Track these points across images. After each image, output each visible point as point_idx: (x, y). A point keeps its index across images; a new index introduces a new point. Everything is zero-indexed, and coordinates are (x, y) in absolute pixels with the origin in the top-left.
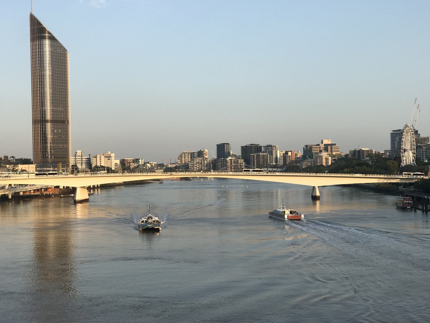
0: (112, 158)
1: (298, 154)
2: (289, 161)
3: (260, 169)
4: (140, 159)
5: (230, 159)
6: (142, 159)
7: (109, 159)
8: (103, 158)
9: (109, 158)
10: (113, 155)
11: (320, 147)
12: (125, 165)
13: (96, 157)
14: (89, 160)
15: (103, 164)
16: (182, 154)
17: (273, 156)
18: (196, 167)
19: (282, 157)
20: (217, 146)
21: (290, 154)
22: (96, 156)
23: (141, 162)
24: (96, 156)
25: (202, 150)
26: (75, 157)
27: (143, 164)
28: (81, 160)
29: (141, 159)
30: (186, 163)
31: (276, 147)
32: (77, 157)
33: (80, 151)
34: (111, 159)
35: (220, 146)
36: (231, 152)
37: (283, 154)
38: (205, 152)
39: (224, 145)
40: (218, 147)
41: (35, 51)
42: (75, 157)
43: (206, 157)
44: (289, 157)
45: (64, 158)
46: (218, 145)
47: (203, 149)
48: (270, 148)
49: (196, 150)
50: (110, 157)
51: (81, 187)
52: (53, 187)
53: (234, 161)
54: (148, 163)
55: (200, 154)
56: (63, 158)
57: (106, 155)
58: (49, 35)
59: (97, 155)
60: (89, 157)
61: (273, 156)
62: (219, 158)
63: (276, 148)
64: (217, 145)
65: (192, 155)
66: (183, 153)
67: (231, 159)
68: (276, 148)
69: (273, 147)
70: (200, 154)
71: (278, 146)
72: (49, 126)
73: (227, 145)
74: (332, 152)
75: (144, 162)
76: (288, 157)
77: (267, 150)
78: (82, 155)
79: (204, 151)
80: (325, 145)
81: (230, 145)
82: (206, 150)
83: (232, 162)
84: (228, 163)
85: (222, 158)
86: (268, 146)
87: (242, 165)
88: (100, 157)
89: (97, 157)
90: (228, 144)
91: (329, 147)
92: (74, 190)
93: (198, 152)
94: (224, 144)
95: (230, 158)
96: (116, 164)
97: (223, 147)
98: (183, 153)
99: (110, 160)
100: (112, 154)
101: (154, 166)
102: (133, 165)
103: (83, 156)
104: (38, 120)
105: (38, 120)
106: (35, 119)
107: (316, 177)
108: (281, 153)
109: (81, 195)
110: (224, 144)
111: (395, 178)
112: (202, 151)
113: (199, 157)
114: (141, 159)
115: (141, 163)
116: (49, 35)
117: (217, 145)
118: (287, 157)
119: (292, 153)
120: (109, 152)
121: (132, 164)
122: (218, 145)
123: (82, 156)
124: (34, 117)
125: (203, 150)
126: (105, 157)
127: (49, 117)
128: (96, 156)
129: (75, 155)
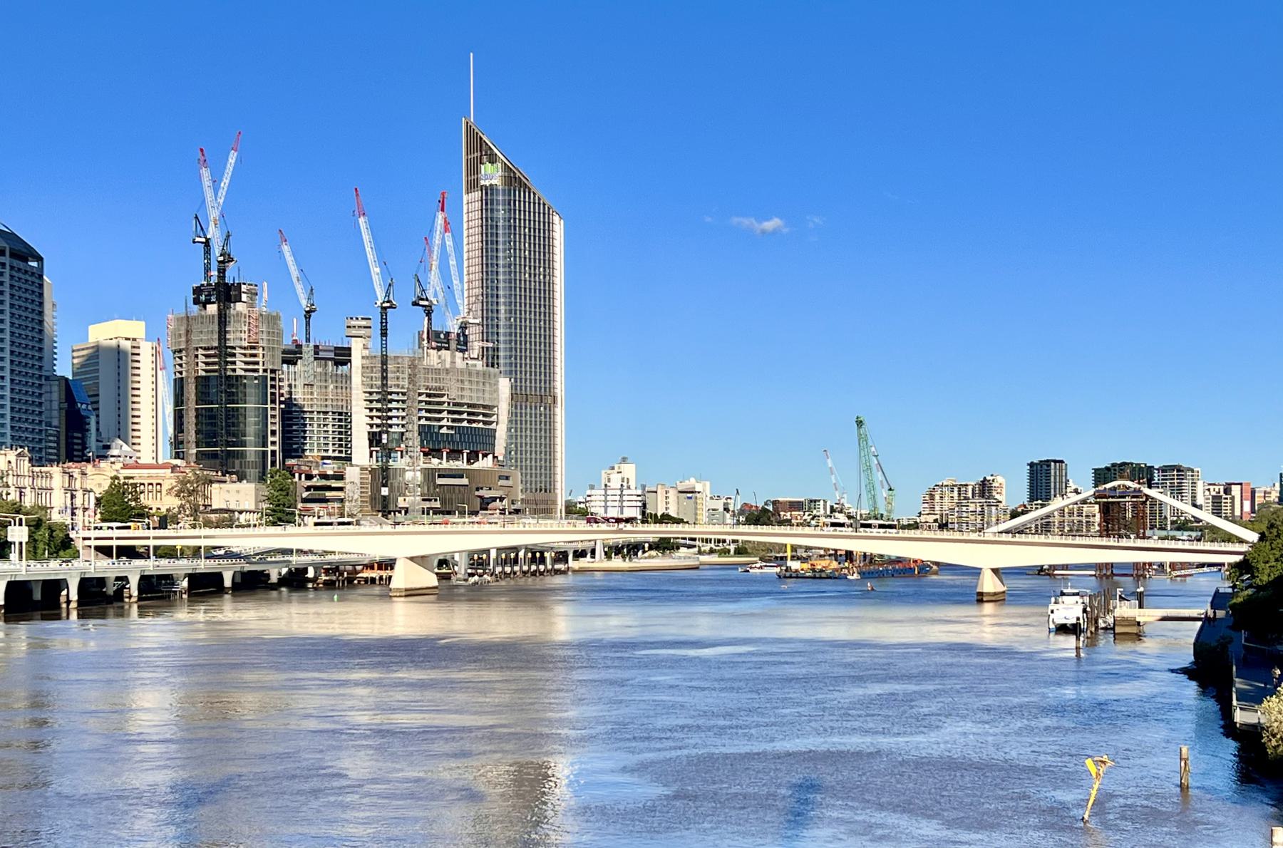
1: (1270, 493)
2: (1229, 511)
4: (819, 501)
7: (690, 498)
14: (640, 498)
15: (673, 513)
17: (1182, 496)
19: (1208, 499)
20: (1028, 467)
21: (1236, 490)
25: (988, 478)
27: (828, 513)
28: (625, 498)
30: (944, 513)
31: (1193, 471)
35: (1039, 467)
36: (1070, 483)
37: (1217, 490)
39: (1049, 466)
42: (606, 490)
43: (997, 496)
44: (1229, 501)
46: (1031, 465)
47: (992, 475)
48: (1176, 476)
50: (692, 492)
51: (412, 559)
61: (1182, 496)
63: (1192, 476)
64: (1028, 464)
68: (1192, 476)
69: (1182, 471)
70: (985, 488)
71: (1199, 469)
73: (1058, 464)
76: (1227, 499)
77: (1166, 480)
78: (622, 485)
79: (993, 481)
82: (1000, 479)
86: (1172, 468)
87: (1092, 519)
90: (1062, 462)
96: (713, 510)
99: (693, 500)
103: (625, 487)
108: (1212, 490)
109: (403, 577)
114: (822, 503)
117: (1028, 464)
118: (1224, 501)
119: (1242, 489)
122: (1031, 465)
125: (991, 478)
129: (606, 485)
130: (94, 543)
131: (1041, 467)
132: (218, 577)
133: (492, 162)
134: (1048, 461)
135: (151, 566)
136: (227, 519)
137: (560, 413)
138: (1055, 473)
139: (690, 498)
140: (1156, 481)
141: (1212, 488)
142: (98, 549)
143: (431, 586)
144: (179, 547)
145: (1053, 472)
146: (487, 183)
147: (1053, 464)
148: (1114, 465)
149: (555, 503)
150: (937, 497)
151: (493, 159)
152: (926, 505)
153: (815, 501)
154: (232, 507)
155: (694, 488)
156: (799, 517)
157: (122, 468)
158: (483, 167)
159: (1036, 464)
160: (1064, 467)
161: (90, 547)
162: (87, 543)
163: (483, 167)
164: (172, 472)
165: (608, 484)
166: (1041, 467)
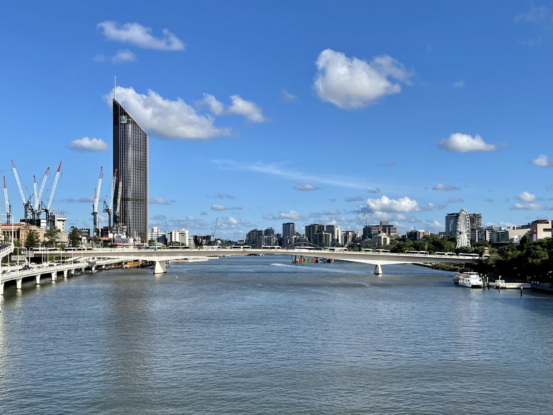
4: (211, 236)
7: (183, 236)
8: (178, 234)
11: (379, 228)
15: (178, 240)
21: (350, 234)
23: (212, 239)
26: (152, 233)
33: (157, 228)
48: (331, 229)
54: (219, 240)
60: (164, 234)
74: (390, 233)
80: (383, 226)
88: (175, 234)
90: (293, 223)
91: (387, 228)
100: (186, 231)
115: (212, 240)
123: (158, 233)
133: (125, 115)
139: (183, 236)
140: (325, 230)
141: (342, 233)
148: (312, 225)
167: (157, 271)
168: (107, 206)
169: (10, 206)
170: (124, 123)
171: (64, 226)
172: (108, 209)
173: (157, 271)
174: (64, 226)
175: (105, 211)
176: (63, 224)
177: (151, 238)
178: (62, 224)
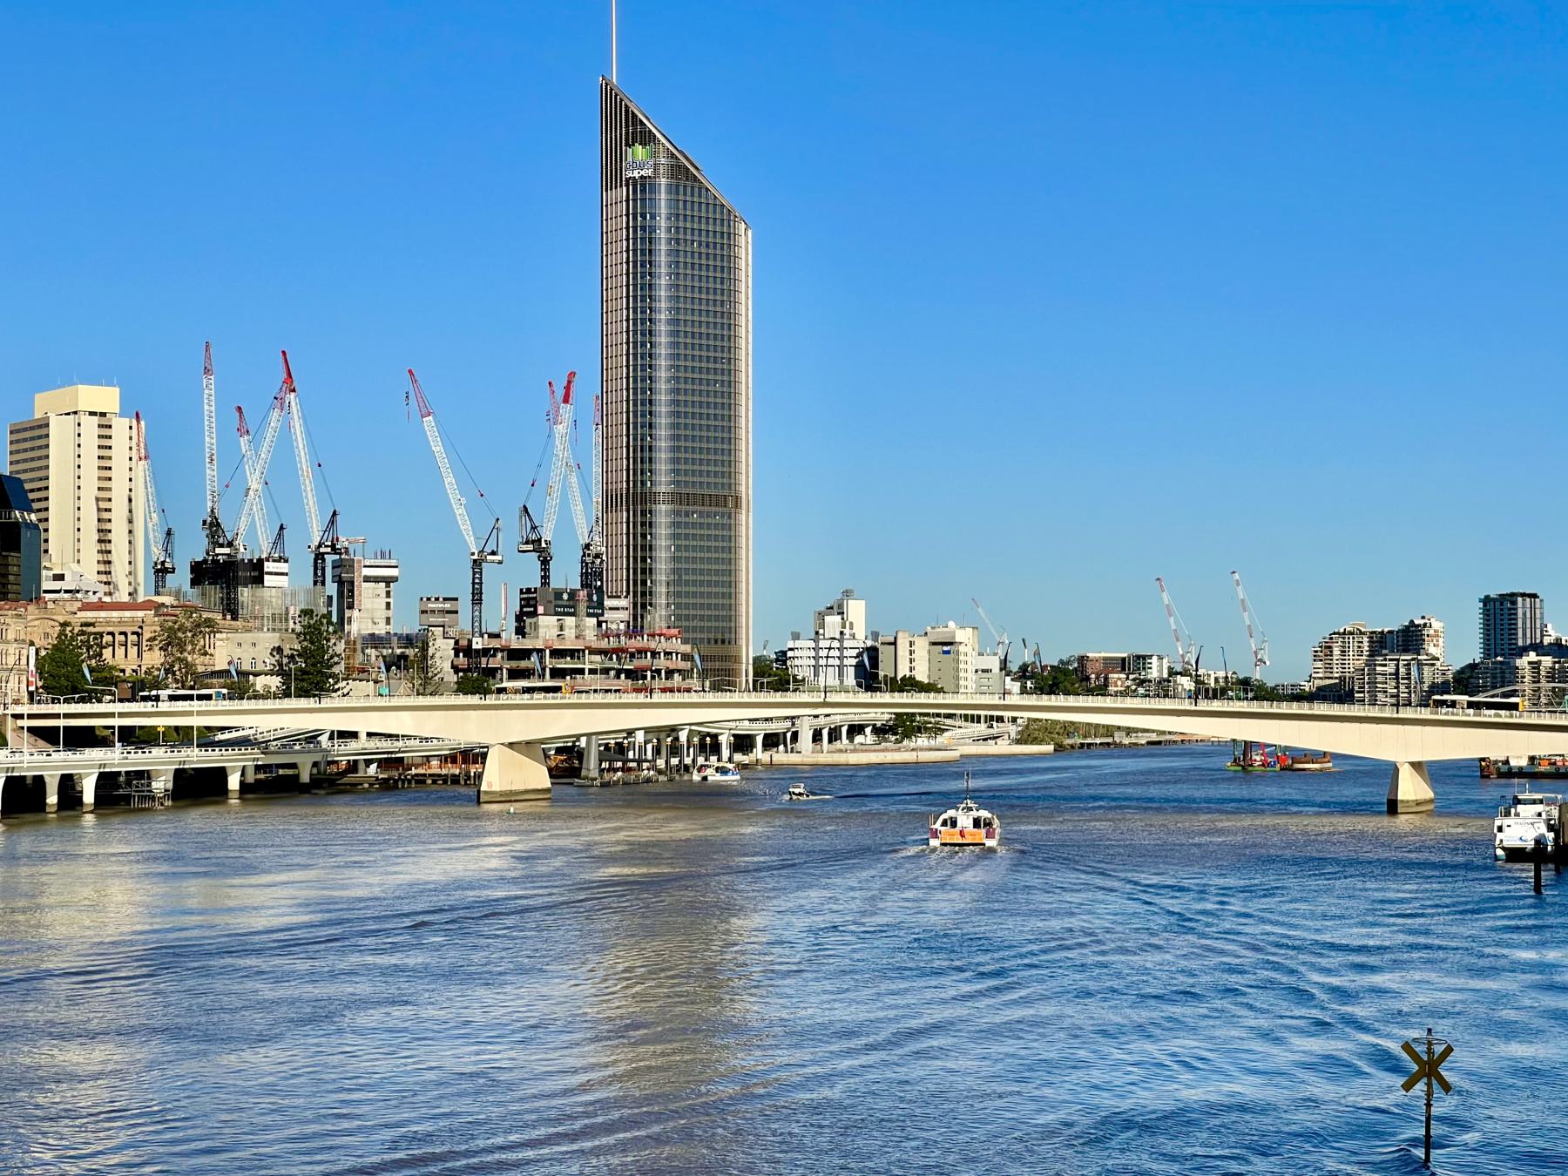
0: (962, 649)
3: (1470, 696)
4: (1150, 657)
5: (1530, 663)
6: (1160, 658)
7: (948, 652)
8: (922, 646)
9: (945, 648)
10: (963, 635)
12: (1088, 679)
13: (894, 643)
15: (922, 676)
16: (1331, 638)
18: (1386, 692)
20: (1481, 605)
22: (893, 640)
23: (1155, 671)
24: (895, 638)
25: (1417, 622)
26: (816, 641)
27: (1165, 675)
29: (1155, 659)
32: (823, 644)
34: (958, 651)
35: (1497, 604)
38: (1432, 632)
39: (1514, 603)
40: (1488, 610)
41: (617, 224)
42: (816, 641)
45: (723, 642)
46: (1486, 601)
47: (1423, 618)
49: (1394, 624)
50: (951, 644)
51: (511, 745)
52: (553, 752)
53: (1548, 672)
55: (1410, 638)
56: (713, 642)
57: (940, 634)
58: (673, 162)
59: (900, 635)
62: (1489, 655)
64: (1480, 600)
65: (1380, 643)
66: (1334, 633)
67: (1536, 663)
70: (1410, 638)
72: (663, 514)
75: (1169, 668)
78: (842, 633)
79: (1425, 625)
81: (1542, 601)
82: (1436, 625)
83: (1539, 673)
84: (1524, 677)
85: (1499, 658)
89: (899, 642)
90: (1534, 596)
92: (474, 756)
93: (1403, 631)
94: (1514, 599)
95: (1532, 656)
96: (983, 671)
97: (1510, 609)
98: (1334, 633)
101: (1213, 685)
102: (1119, 679)
103: (847, 636)
104: (621, 495)
105: (621, 495)
106: (612, 490)
107: (1357, 725)
109: (496, 776)
110: (1512, 597)
111: (1355, 717)
112: (1419, 625)
113: (1406, 651)
114: (1155, 658)
116: (673, 162)
117: (1480, 600)
120: (952, 624)
121: (1116, 676)
122: (1486, 601)
123: (841, 640)
124: (607, 483)
125: (1422, 622)
126: (934, 644)
127: (663, 483)
128: (893, 640)
129: (817, 633)
130: (26, 723)
131: (1502, 604)
132: (220, 774)
133: (644, 144)
134: (1513, 595)
135: (116, 758)
136: (238, 685)
137: (747, 524)
138: (1525, 614)
139: (948, 652)
142: (31, 730)
143: (540, 787)
144: (161, 730)
145: (1520, 612)
146: (636, 174)
147: (1520, 599)
149: (737, 659)
150: (1336, 651)
151: (647, 138)
152: (1319, 664)
153: (1144, 657)
154: (246, 667)
155: (954, 637)
156: (1119, 683)
157: (80, 610)
158: (630, 150)
159: (1494, 600)
160: (1538, 605)
161: (23, 728)
162: (20, 723)
163: (630, 150)
164: (156, 615)
165: (821, 631)
166: (1502, 604)
167: (490, 784)
168: (534, 528)
169: (169, 533)
170: (642, 177)
171: (390, 613)
172: (540, 540)
173: (490, 784)
174: (390, 613)
175: (525, 547)
176: (388, 604)
177: (813, 662)
178: (384, 606)
